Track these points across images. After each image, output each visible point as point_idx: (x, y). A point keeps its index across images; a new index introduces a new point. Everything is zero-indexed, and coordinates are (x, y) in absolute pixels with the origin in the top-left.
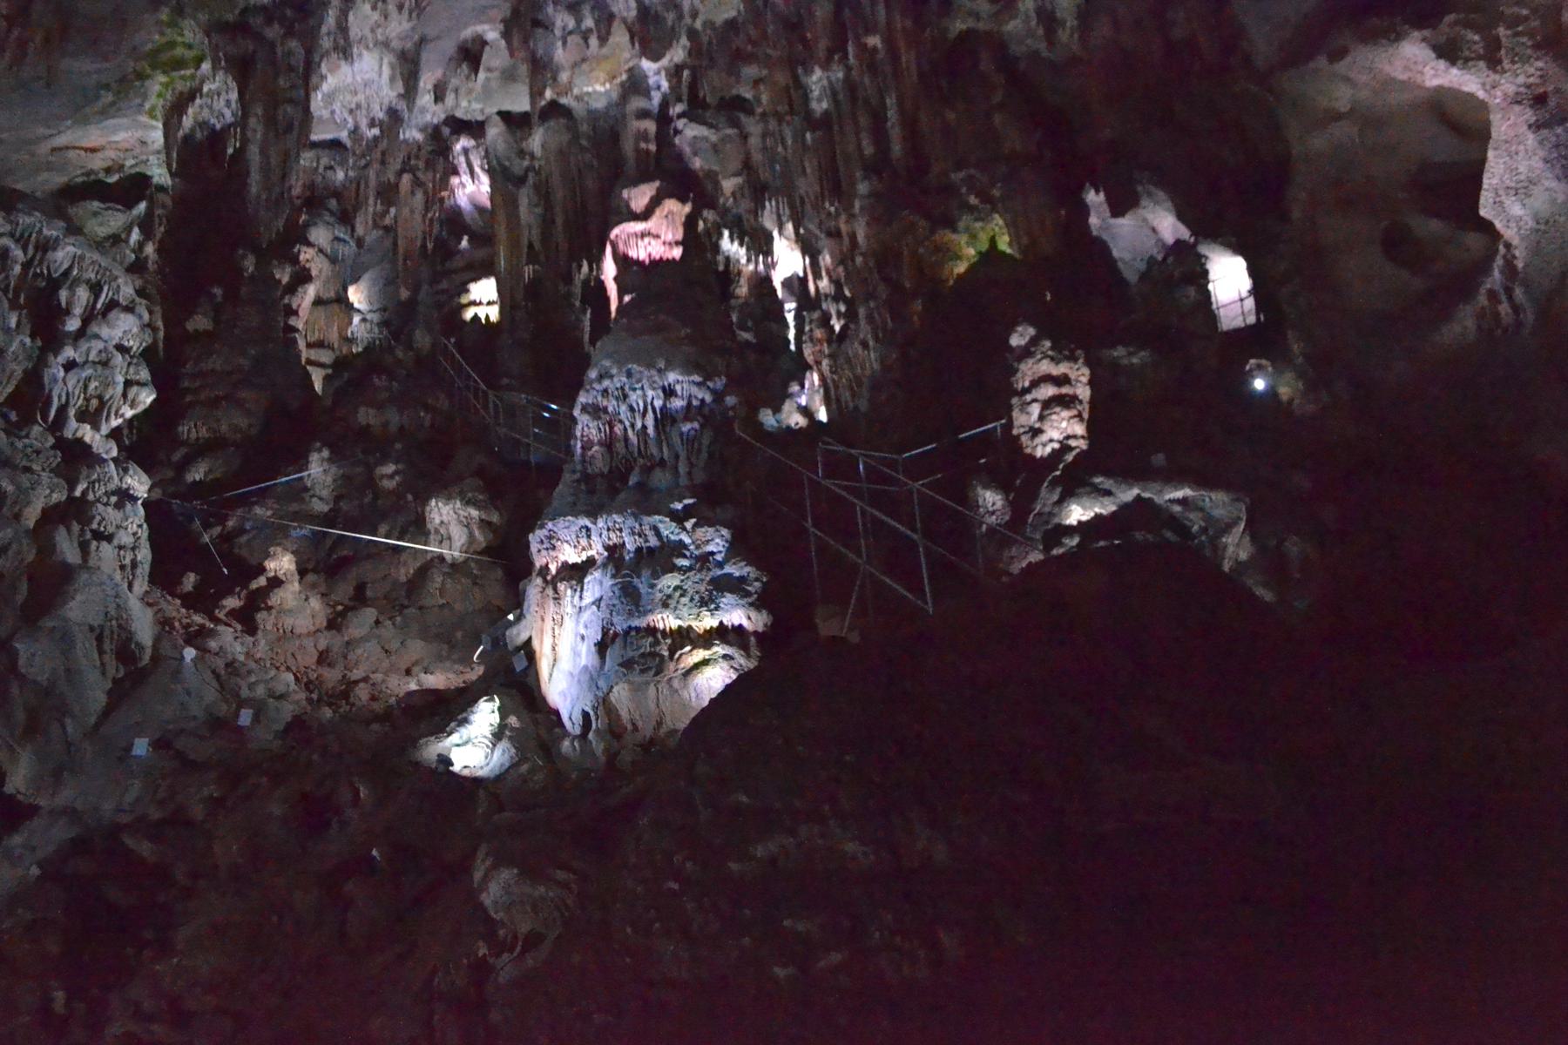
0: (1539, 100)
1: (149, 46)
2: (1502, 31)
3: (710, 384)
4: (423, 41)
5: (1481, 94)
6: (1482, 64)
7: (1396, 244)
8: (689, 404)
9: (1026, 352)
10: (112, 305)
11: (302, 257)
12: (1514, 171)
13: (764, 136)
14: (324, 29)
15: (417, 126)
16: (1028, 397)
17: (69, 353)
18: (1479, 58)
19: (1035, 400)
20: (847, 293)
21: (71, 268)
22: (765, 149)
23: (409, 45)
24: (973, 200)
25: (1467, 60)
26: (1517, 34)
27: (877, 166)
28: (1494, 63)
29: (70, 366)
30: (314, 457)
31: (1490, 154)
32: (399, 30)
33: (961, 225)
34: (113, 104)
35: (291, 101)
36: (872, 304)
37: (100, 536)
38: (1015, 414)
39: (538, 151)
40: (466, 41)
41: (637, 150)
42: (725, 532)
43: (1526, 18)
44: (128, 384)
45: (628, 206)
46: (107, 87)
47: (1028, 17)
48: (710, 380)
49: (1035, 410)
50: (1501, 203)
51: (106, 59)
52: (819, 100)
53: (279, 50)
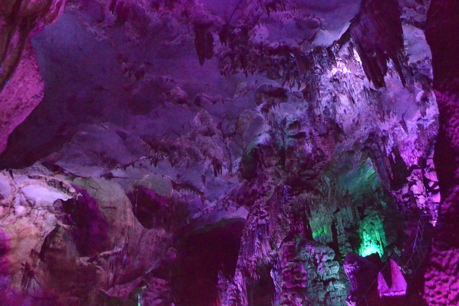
1: (359, 159)
3: (353, 265)
4: (403, 115)
8: (351, 271)
10: (324, 254)
11: (409, 180)
14: (380, 135)
15: (431, 119)
17: (319, 267)
21: (315, 252)
23: (401, 119)
29: (320, 269)
30: (395, 249)
32: (395, 119)
34: (364, 170)
35: (379, 157)
37: (334, 298)
40: (422, 97)
42: (355, 303)
44: (330, 267)
46: (359, 169)
48: (353, 263)
51: (352, 169)
53: (372, 148)
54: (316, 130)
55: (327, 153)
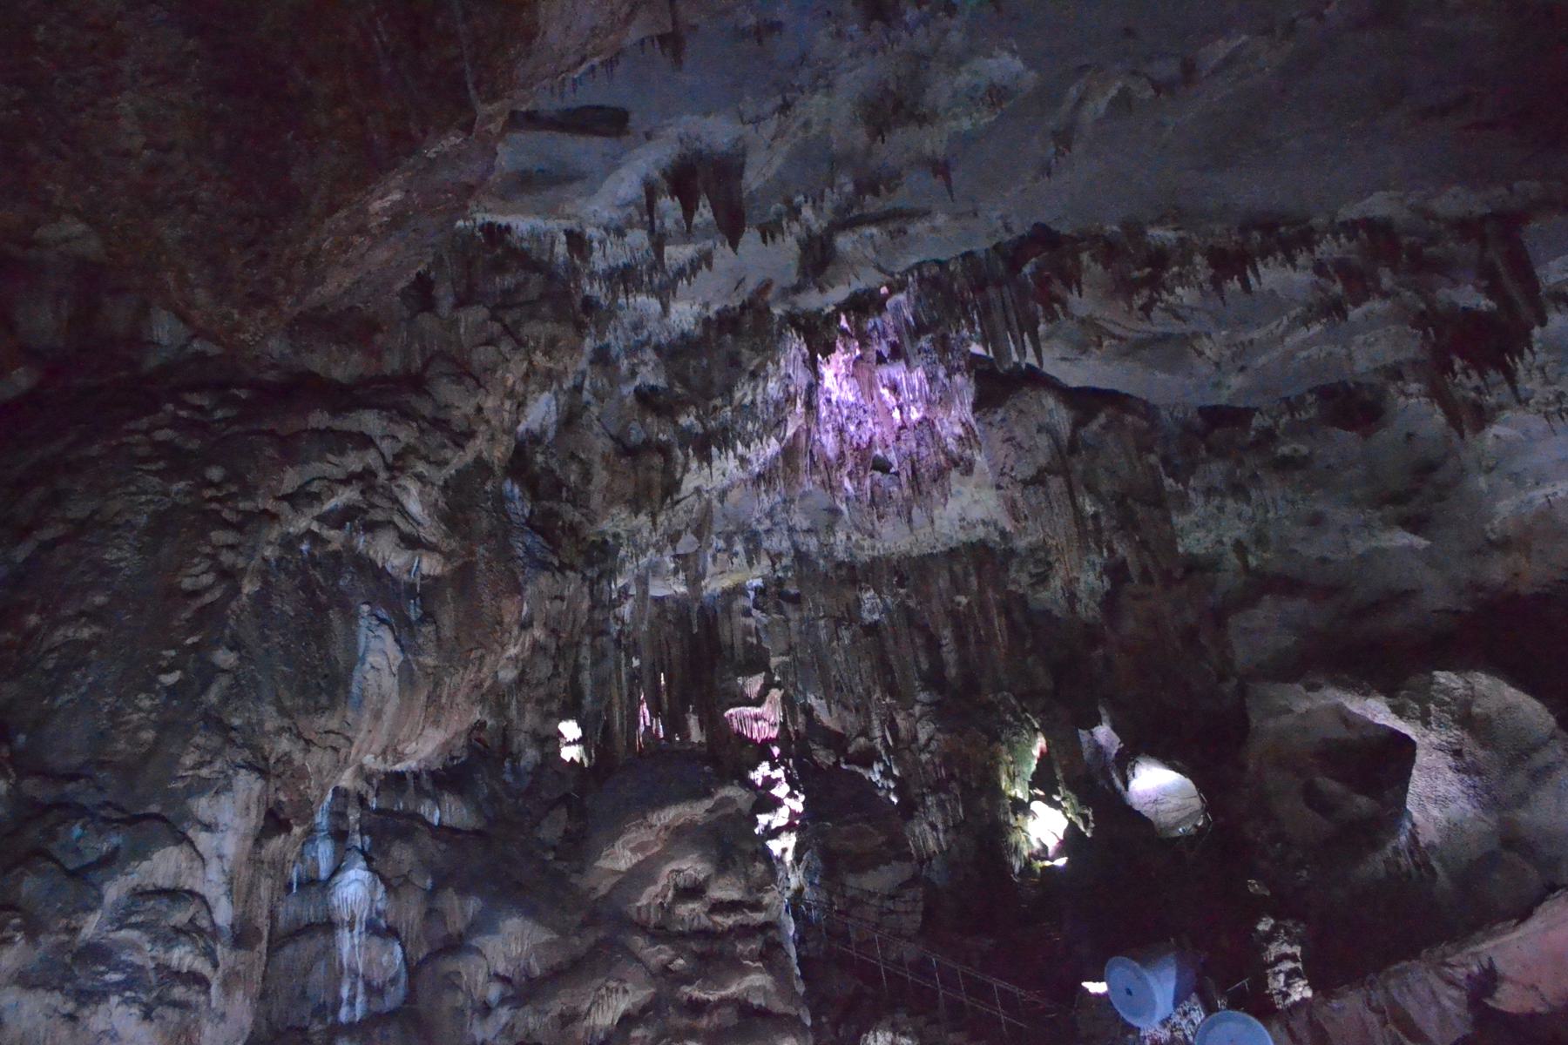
0: (1457, 754)
2: (1432, 706)
5: (1414, 738)
6: (1419, 722)
7: (1312, 796)
9: (1270, 937)
12: (1434, 789)
13: (802, 620)
16: (1277, 969)
18: (1417, 718)
19: (1280, 972)
20: (896, 772)
22: (800, 632)
24: (1009, 717)
25: (1409, 718)
26: (1443, 711)
27: (935, 679)
28: (1426, 724)
31: (1414, 772)
33: (1003, 737)
36: (943, 796)
38: (1270, 980)
39: (627, 618)
41: (745, 642)
43: (1449, 703)
45: (742, 692)
47: (1056, 592)
49: (1282, 978)
50: (1424, 806)
52: (871, 611)
54: (599, 396)
55: (596, 501)
